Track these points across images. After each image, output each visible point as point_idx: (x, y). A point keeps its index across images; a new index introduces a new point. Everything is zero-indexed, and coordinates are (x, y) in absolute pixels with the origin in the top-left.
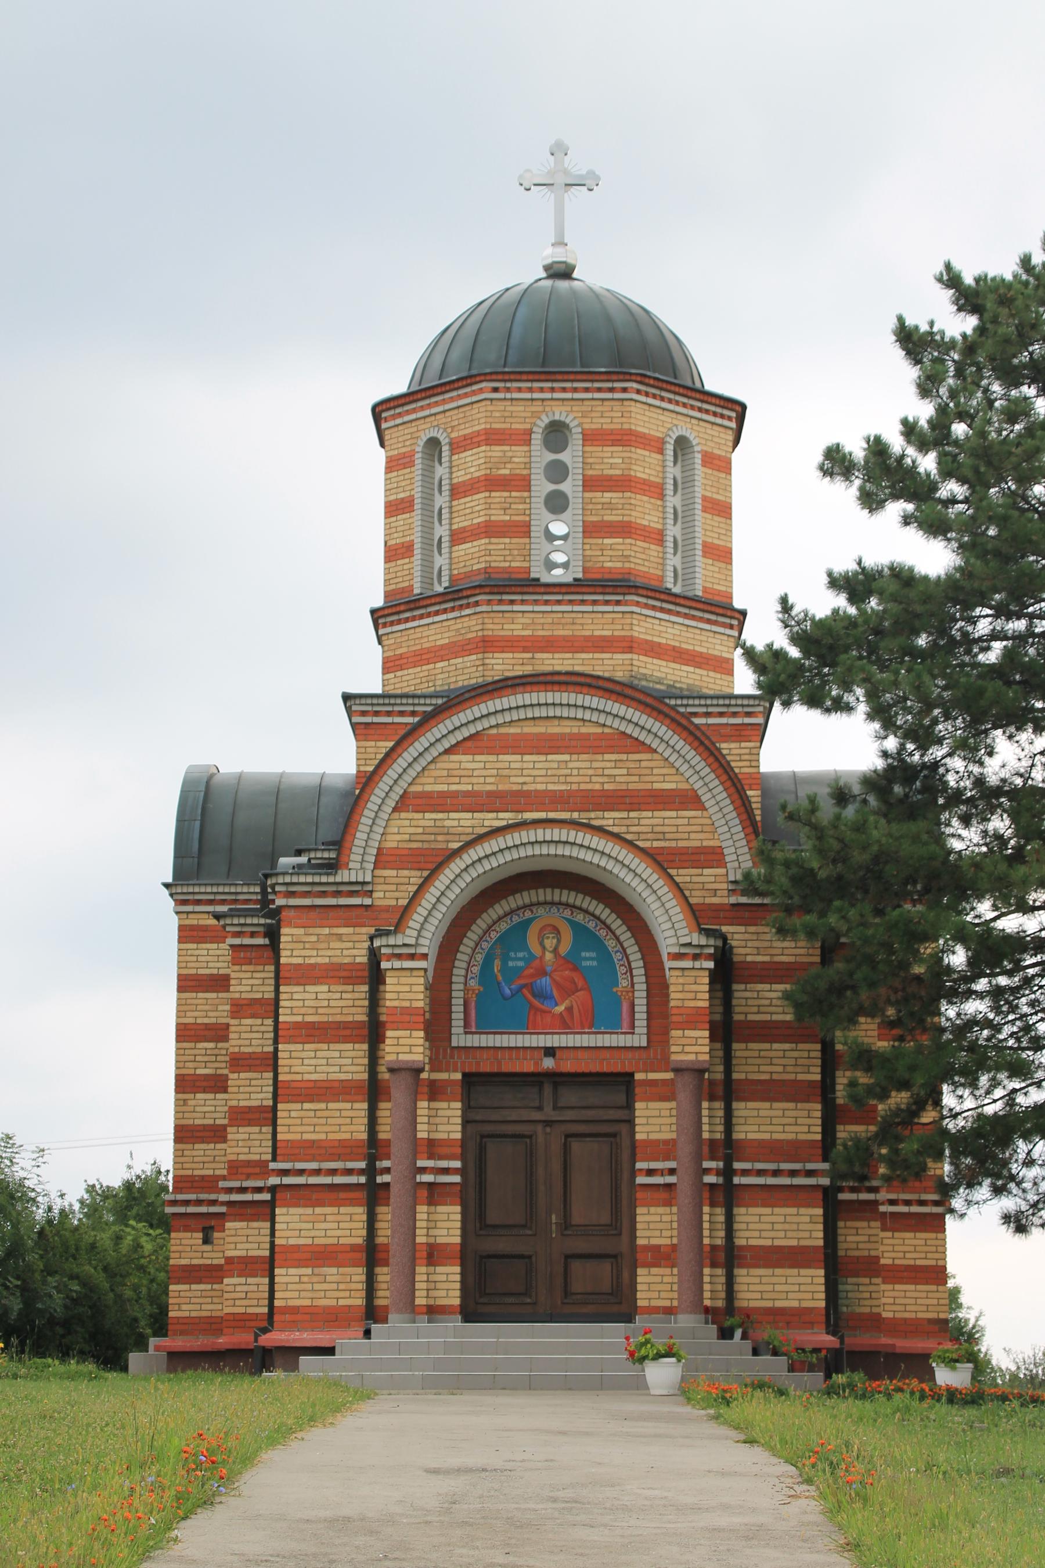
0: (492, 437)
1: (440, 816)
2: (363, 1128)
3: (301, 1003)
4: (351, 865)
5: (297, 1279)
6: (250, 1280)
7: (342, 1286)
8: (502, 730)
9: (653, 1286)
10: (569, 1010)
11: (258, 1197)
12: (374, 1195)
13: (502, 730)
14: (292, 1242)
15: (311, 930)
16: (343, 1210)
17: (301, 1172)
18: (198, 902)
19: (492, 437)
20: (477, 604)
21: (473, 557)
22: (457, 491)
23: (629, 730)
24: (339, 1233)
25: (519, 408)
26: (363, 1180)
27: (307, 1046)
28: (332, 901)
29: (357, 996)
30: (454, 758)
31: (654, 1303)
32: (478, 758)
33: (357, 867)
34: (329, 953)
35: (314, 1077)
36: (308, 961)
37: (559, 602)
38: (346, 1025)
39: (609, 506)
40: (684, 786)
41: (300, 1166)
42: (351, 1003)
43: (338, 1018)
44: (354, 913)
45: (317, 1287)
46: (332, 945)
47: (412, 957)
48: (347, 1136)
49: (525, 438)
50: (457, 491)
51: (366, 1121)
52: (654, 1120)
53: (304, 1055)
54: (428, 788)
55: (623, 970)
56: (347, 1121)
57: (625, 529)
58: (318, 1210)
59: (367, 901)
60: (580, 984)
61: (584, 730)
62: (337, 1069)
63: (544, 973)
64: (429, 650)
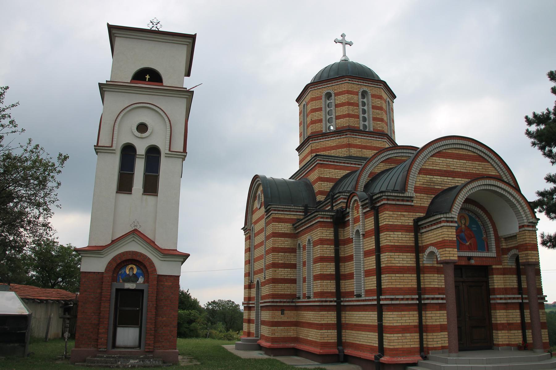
0: (348, 92)
1: (431, 177)
3: (393, 238)
4: (408, 191)
5: (397, 338)
6: (329, 331)
7: (412, 340)
8: (447, 151)
9: (501, 337)
10: (470, 244)
11: (331, 304)
12: (421, 308)
13: (447, 151)
14: (395, 324)
15: (395, 213)
16: (411, 313)
17: (397, 299)
18: (279, 211)
19: (348, 92)
20: (347, 135)
21: (344, 122)
22: (337, 106)
23: (482, 154)
24: (409, 321)
25: (355, 86)
26: (417, 302)
27: (396, 254)
28: (402, 203)
29: (411, 236)
31: (504, 343)
32: (441, 159)
33: (410, 192)
34: (401, 221)
35: (399, 265)
36: (395, 223)
37: (367, 137)
38: (408, 247)
40: (498, 174)
41: (397, 297)
42: (409, 239)
45: (404, 341)
46: (402, 218)
47: (452, 222)
48: (410, 286)
49: (357, 93)
50: (337, 106)
51: (416, 281)
52: (498, 281)
53: (395, 257)
54: (427, 167)
55: (484, 232)
56: (410, 281)
57: (382, 120)
58: (403, 313)
59: (412, 204)
61: (469, 153)
62: (406, 262)
63: (463, 232)
64: (328, 147)
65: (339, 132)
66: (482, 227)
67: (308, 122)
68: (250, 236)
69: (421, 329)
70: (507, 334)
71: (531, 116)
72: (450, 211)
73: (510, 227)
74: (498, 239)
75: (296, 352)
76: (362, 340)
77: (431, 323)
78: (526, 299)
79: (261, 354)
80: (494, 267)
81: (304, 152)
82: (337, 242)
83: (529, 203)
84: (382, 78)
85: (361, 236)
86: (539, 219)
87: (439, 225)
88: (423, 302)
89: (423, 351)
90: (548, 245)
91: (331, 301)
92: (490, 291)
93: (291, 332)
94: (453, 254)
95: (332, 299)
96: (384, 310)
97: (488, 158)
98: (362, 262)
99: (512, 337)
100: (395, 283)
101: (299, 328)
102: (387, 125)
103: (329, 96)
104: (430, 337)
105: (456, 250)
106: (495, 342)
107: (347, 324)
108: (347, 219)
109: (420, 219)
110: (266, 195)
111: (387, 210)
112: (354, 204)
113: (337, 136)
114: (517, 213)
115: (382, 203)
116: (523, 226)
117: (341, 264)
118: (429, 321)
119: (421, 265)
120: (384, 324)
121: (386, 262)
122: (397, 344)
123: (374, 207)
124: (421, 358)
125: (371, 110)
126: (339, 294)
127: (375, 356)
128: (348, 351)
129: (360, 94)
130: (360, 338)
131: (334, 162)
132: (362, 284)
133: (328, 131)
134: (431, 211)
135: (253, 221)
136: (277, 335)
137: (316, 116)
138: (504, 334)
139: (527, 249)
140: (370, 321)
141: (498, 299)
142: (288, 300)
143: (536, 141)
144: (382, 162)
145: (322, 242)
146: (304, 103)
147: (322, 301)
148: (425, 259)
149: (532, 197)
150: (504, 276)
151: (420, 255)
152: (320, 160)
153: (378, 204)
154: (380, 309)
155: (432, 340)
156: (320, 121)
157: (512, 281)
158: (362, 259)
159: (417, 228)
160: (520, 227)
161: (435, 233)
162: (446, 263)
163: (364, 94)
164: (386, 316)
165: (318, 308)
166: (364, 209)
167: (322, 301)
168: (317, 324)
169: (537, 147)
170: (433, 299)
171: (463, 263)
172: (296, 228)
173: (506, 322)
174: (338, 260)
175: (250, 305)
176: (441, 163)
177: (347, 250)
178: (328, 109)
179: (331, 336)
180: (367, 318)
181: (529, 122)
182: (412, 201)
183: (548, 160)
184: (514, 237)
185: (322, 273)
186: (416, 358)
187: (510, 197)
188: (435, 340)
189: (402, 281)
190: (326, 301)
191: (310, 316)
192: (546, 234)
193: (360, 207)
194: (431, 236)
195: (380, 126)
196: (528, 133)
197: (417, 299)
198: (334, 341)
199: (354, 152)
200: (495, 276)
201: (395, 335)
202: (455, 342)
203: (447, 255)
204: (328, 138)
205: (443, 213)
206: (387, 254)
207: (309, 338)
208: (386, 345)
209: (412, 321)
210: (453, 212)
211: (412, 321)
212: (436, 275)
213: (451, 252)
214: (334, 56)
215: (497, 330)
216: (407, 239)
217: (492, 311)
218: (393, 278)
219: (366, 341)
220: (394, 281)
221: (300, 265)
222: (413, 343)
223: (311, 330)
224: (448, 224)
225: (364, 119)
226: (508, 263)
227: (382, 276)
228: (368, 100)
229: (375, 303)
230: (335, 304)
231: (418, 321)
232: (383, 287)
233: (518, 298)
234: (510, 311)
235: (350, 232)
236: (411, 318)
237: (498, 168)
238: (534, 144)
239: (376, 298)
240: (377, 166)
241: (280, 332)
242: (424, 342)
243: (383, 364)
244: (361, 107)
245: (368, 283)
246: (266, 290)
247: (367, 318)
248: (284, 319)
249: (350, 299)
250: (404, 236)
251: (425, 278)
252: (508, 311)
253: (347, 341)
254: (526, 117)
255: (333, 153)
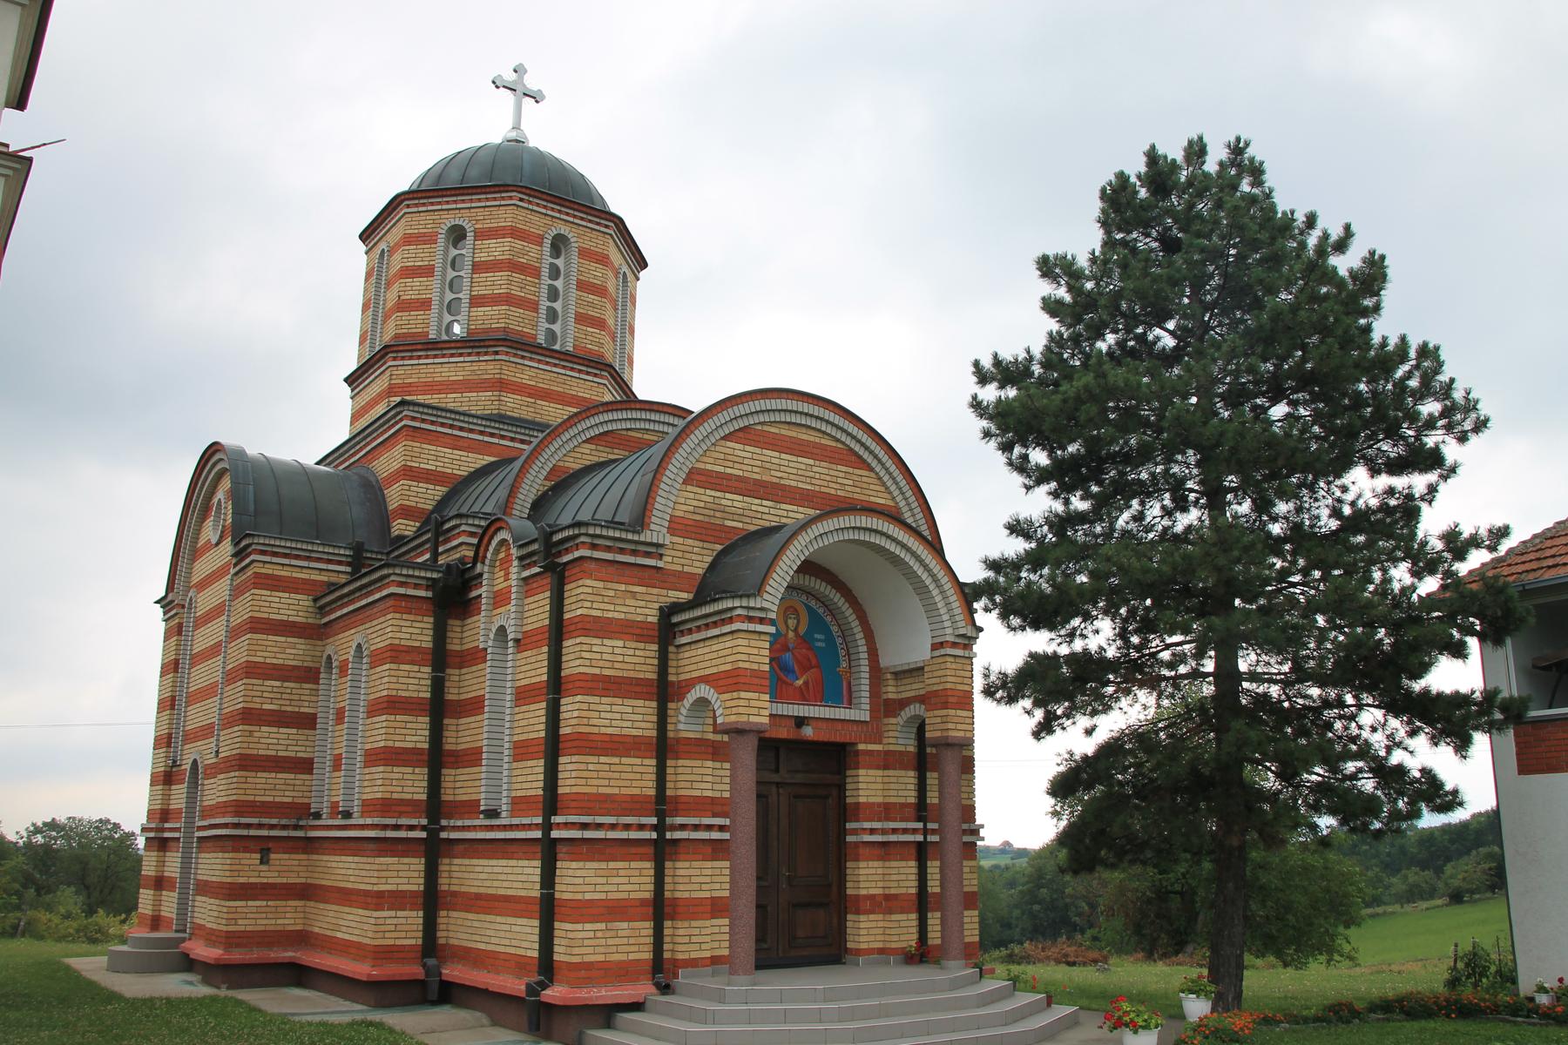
0: (515, 233)
1: (718, 494)
2: (650, 784)
3: (598, 656)
4: (652, 526)
6: (400, 913)
7: (632, 941)
8: (766, 428)
9: (865, 931)
10: (806, 683)
11: (412, 834)
12: (662, 851)
13: (766, 428)
14: (588, 896)
15: (610, 585)
17: (599, 826)
18: (275, 554)
19: (515, 233)
20: (497, 353)
21: (492, 317)
22: (477, 267)
23: (857, 448)
25: (535, 218)
26: (654, 835)
27: (604, 700)
28: (631, 559)
29: (648, 654)
30: (729, 444)
32: (748, 448)
33: (657, 532)
34: (624, 609)
35: (610, 731)
37: (555, 365)
38: (639, 682)
39: (591, 304)
40: (890, 503)
41: (599, 820)
43: (632, 674)
44: (647, 573)
45: (610, 942)
46: (628, 602)
47: (761, 621)
48: (637, 791)
49: (539, 240)
50: (477, 267)
51: (654, 777)
53: (601, 708)
54: (709, 467)
56: (636, 776)
57: (600, 324)
58: (612, 865)
59: (660, 564)
60: (814, 662)
62: (629, 724)
64: (441, 383)
65: (475, 343)
66: (839, 641)
67: (390, 305)
68: (180, 626)
69: (660, 909)
70: (881, 924)
71: (987, 363)
72: (759, 590)
73: (909, 645)
74: (876, 671)
75: (299, 975)
76: (493, 940)
77: (686, 895)
78: (934, 832)
79: (191, 983)
80: (861, 747)
81: (368, 389)
82: (441, 658)
83: (962, 586)
84: (613, 210)
85: (511, 644)
86: (981, 630)
87: (727, 629)
88: (668, 835)
89: (662, 971)
90: (998, 695)
91: (411, 828)
92: (846, 812)
93: (288, 916)
94: (756, 709)
95: (414, 822)
96: (560, 856)
97: (870, 459)
98: (508, 718)
99: (893, 931)
100: (595, 782)
101: (312, 904)
102: (614, 339)
103: (457, 235)
104: (681, 932)
105: (767, 697)
106: (849, 945)
107: (454, 894)
108: (474, 594)
109: (676, 608)
110: (239, 506)
111: (590, 577)
112: (497, 551)
113: (469, 354)
114: (931, 609)
115: (577, 554)
116: (941, 645)
117: (446, 721)
118: (681, 887)
119: (671, 735)
120: (557, 895)
121: (574, 722)
122: (591, 950)
123: (552, 563)
124: (653, 990)
125: (574, 293)
126: (435, 806)
127: (528, 986)
128: (453, 972)
129: (547, 243)
130: (488, 932)
131: (451, 427)
132: (501, 780)
133: (445, 337)
134: (708, 589)
135: (195, 579)
136: (243, 925)
137: (414, 288)
138: (873, 924)
139: (945, 706)
140: (520, 885)
141: (863, 831)
142: (284, 822)
143: (993, 429)
144: (587, 441)
145: (396, 654)
146: (383, 246)
147: (385, 827)
148: (682, 718)
149: (971, 571)
150: (887, 772)
151: (671, 705)
152: (413, 419)
153: (566, 559)
154: (549, 853)
155: (686, 939)
156: (425, 304)
157: (902, 786)
158: (508, 711)
159: (666, 631)
160: (935, 647)
161: (715, 648)
162: (737, 731)
163: (559, 244)
164: (565, 872)
165: (372, 846)
166: (525, 567)
167: (385, 827)
168: (366, 893)
169: (993, 444)
170: (696, 827)
171: (783, 733)
172: (322, 611)
173: (880, 891)
174: (439, 708)
175: (167, 835)
176: (748, 460)
177: (464, 684)
178: (451, 274)
179: (406, 927)
180: (511, 877)
181: (983, 378)
182: (661, 556)
183: (1018, 479)
184: (918, 671)
185: (390, 744)
186: (643, 989)
187: (916, 567)
188: (694, 939)
189: (616, 775)
190: (397, 827)
191: (346, 870)
192: (995, 669)
193: (515, 563)
194: (700, 657)
195: (595, 340)
196: (976, 405)
197: (654, 828)
198: (413, 942)
199: (513, 405)
200: (862, 772)
201: (588, 926)
202: (748, 945)
203: (741, 710)
204: (443, 356)
205: (741, 597)
206: (579, 698)
207: (339, 935)
208: (560, 954)
209: (637, 887)
210: (766, 596)
211: (637, 887)
212: (709, 764)
213: (753, 703)
214: (483, 125)
215: (858, 912)
216: (638, 659)
217: (849, 864)
218: (591, 767)
219: (507, 942)
220: (595, 775)
221: (326, 719)
222: (635, 948)
223: (347, 909)
224: (752, 627)
225: (552, 316)
226: (899, 738)
227: (562, 760)
228: (568, 264)
229: (538, 834)
230: (424, 835)
231: (652, 887)
232: (561, 791)
233: (915, 831)
234: (894, 864)
235: (478, 630)
236: (633, 880)
237: (893, 488)
238: (987, 434)
239: (539, 820)
240: (570, 452)
241: (255, 916)
242: (666, 947)
243: (550, 1007)
244: (546, 280)
245: (520, 779)
246: (217, 790)
247: (511, 877)
248: (268, 875)
249: (468, 823)
250: (631, 652)
251: (680, 770)
252: (887, 864)
253: (452, 942)
254: (976, 364)
255: (451, 400)
